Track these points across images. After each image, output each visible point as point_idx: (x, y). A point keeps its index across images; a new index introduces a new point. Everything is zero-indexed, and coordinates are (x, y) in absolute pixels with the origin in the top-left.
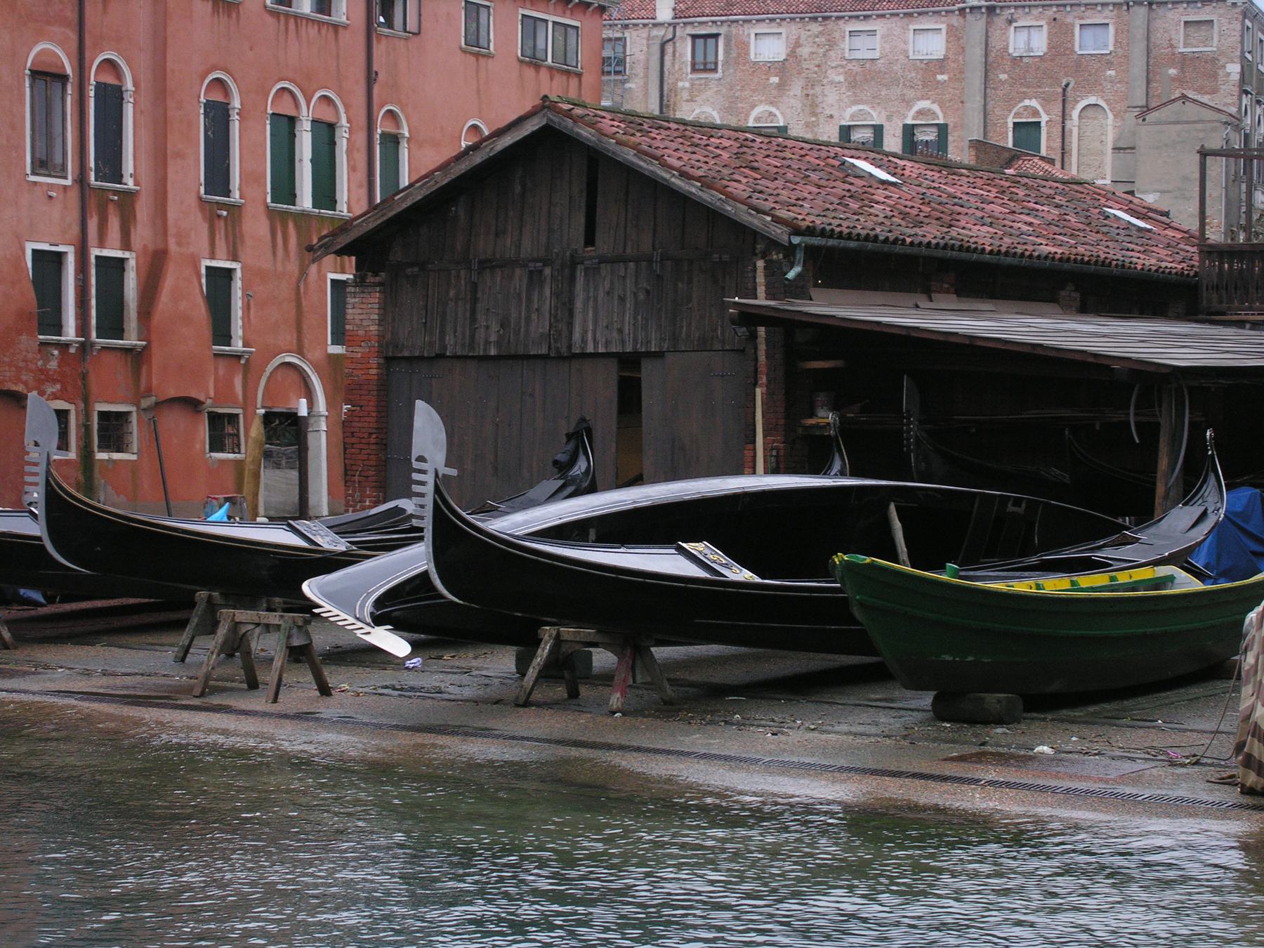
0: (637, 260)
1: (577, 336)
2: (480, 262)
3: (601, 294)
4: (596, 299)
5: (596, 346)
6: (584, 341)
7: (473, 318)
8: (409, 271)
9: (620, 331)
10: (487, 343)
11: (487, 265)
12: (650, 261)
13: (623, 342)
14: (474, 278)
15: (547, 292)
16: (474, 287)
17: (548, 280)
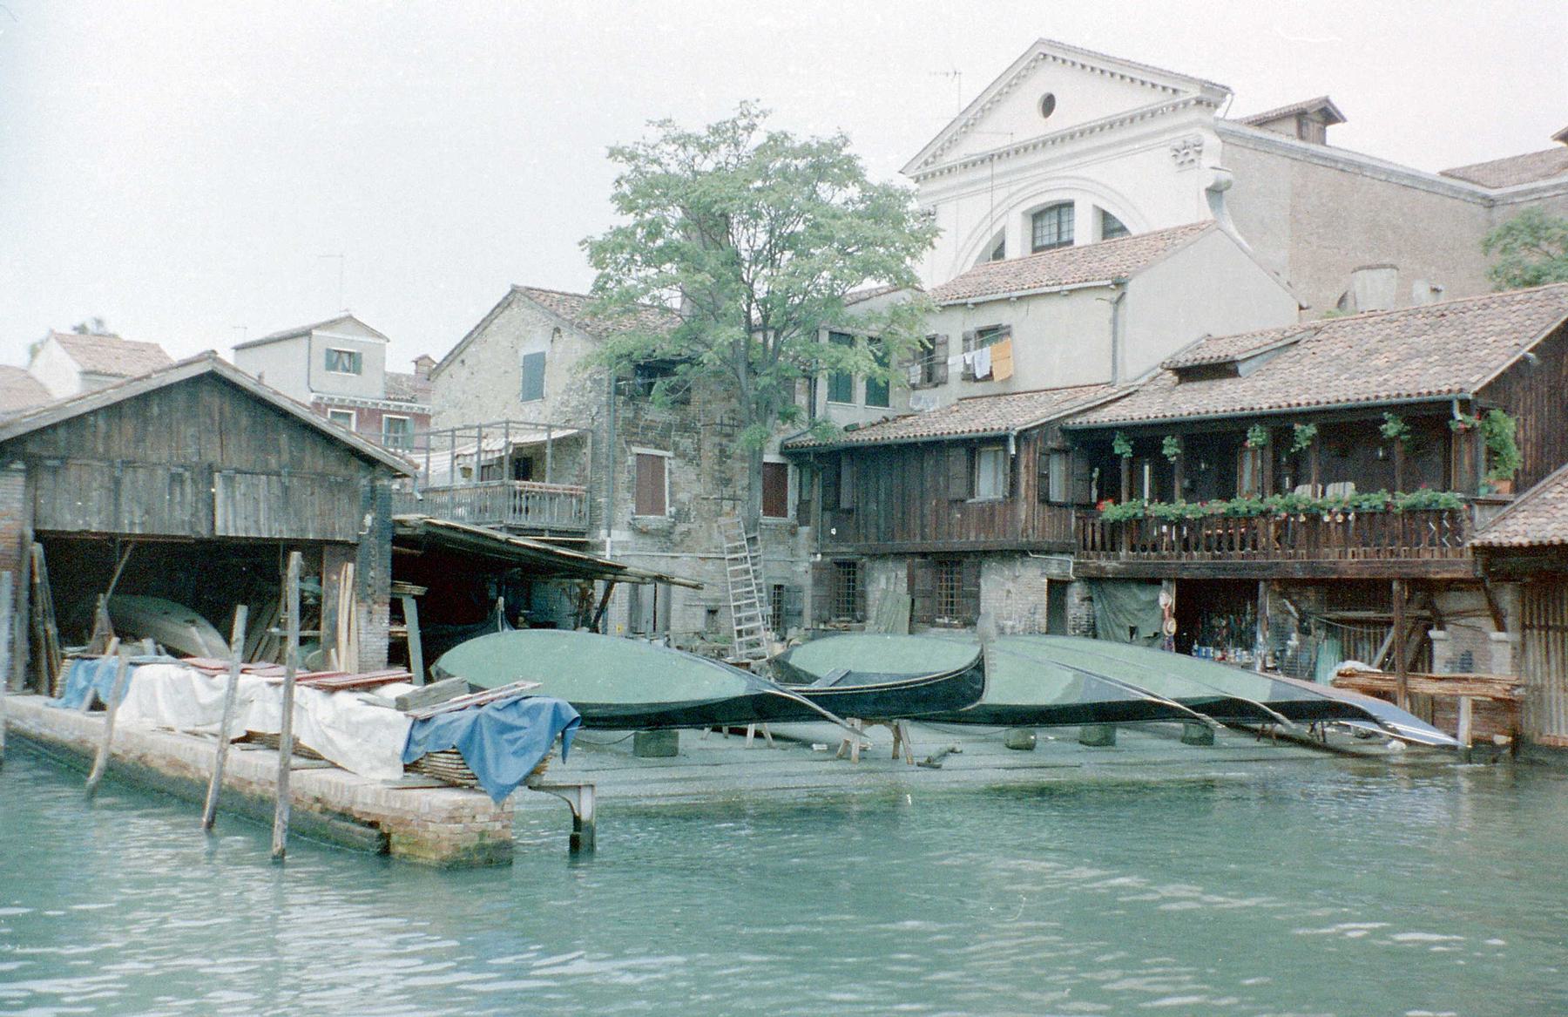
0: (268, 474)
1: (219, 523)
2: (123, 462)
3: (238, 497)
4: (233, 498)
5: (236, 530)
6: (226, 527)
7: (117, 505)
8: (49, 463)
9: (257, 522)
10: (132, 524)
11: (128, 464)
12: (279, 475)
13: (259, 530)
14: (117, 473)
15: (188, 489)
16: (117, 482)
17: (189, 482)
